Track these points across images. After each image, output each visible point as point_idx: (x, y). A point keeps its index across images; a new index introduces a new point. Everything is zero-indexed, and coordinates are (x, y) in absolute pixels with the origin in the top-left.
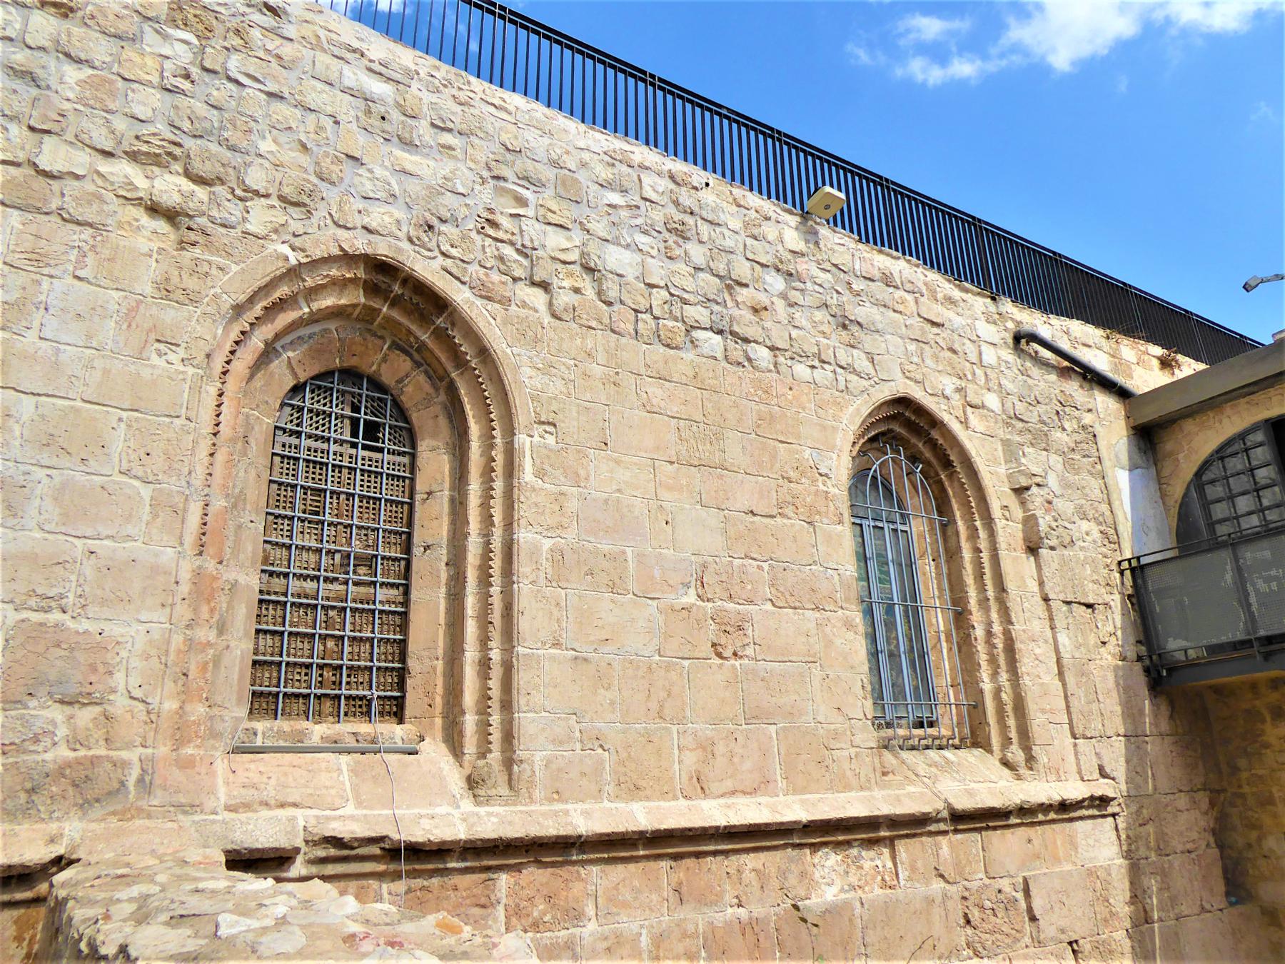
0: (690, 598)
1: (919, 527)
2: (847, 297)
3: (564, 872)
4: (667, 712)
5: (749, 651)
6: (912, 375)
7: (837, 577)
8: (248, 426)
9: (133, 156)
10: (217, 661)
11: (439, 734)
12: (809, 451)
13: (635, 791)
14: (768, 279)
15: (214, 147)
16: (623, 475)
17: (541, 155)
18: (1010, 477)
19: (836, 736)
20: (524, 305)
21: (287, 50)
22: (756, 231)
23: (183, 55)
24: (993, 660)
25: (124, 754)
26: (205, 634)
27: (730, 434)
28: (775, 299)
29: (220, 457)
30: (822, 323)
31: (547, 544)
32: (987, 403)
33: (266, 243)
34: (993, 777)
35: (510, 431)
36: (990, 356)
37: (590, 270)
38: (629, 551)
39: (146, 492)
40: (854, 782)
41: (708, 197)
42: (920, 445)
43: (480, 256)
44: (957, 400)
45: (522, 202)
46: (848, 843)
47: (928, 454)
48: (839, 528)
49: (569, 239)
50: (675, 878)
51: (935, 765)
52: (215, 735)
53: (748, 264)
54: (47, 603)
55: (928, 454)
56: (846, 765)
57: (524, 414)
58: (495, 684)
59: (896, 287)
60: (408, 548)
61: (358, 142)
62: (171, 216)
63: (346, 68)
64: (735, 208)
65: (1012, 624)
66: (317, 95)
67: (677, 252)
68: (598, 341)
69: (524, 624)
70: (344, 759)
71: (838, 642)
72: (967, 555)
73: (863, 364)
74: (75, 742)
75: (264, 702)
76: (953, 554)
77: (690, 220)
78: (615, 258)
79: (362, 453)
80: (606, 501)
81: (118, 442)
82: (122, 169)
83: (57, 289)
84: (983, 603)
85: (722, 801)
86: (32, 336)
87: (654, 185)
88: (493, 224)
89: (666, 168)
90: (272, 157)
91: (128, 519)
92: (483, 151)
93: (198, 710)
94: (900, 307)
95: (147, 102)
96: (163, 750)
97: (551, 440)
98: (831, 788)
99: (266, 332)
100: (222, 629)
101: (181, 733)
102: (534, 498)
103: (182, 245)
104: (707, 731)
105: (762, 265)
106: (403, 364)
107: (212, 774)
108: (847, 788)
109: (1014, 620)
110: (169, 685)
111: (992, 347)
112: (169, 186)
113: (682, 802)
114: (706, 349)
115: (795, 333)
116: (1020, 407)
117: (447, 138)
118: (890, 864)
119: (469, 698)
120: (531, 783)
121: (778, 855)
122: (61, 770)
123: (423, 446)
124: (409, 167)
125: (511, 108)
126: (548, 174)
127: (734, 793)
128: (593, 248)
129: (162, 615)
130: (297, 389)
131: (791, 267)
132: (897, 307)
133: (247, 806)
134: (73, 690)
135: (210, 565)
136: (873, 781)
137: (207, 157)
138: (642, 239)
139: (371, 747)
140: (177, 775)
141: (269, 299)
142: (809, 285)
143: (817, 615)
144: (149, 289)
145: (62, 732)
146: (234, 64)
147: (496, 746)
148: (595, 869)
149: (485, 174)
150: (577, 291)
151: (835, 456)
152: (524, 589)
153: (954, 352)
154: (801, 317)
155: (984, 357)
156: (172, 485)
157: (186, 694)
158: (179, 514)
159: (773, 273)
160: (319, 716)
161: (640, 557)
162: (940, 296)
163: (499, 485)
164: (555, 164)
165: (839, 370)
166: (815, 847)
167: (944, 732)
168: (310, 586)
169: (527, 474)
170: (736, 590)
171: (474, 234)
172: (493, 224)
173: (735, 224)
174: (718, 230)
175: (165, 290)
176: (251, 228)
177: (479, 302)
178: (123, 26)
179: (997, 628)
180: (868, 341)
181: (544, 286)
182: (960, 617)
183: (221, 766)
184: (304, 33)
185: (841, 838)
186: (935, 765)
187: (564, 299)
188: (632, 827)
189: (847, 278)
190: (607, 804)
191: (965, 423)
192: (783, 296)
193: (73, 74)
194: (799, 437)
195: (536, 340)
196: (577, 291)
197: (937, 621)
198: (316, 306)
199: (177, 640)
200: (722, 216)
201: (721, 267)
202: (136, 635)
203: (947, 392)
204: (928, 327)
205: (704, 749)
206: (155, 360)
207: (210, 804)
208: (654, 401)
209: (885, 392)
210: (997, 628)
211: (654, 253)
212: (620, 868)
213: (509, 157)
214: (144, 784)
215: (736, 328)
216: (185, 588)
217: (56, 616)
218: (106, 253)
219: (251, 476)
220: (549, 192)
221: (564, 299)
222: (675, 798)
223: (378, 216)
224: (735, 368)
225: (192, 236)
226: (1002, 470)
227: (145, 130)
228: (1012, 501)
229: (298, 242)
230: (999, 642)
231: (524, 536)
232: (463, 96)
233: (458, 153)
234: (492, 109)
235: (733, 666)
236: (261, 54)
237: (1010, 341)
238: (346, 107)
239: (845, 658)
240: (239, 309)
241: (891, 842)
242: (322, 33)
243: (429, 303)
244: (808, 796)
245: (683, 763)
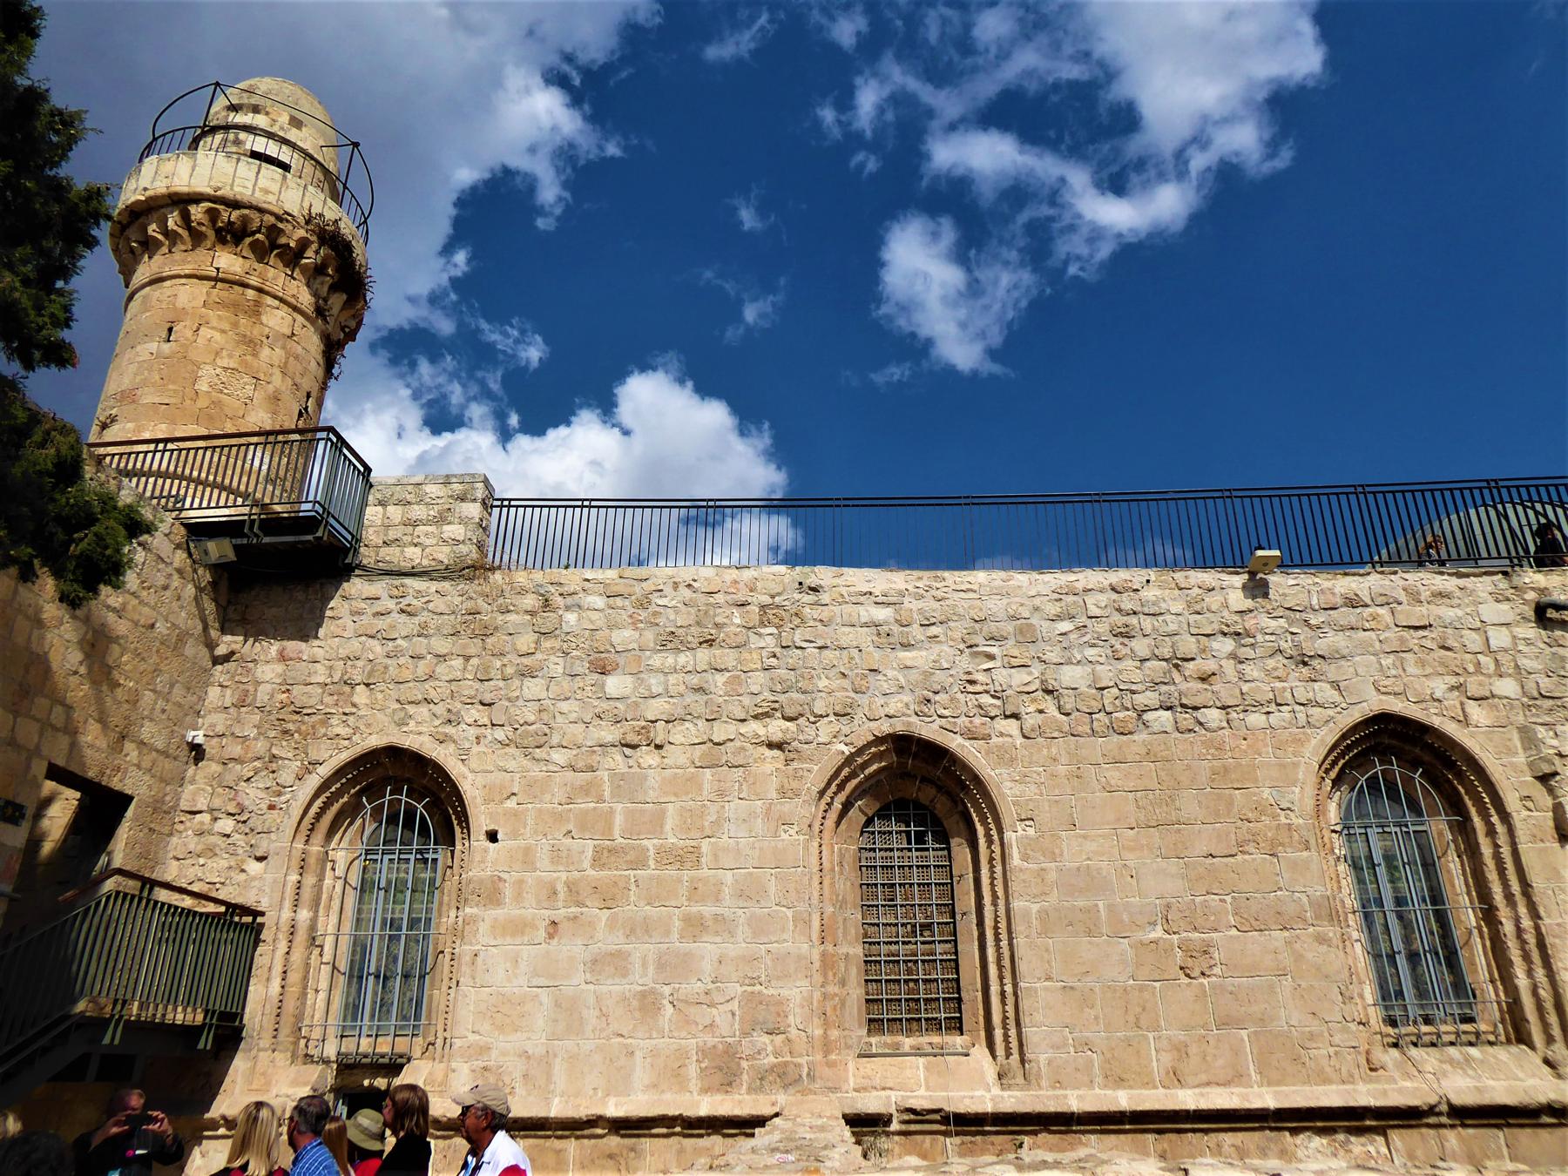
0: (1158, 933)
1: (1439, 827)
2: (1304, 633)
3: (1069, 1137)
4: (1143, 1023)
5: (1217, 970)
6: (1389, 690)
7: (1305, 899)
8: (842, 856)
9: (756, 717)
10: (843, 1003)
11: (984, 1043)
12: (1268, 791)
13: (1120, 1082)
14: (1215, 645)
15: (795, 695)
16: (1091, 846)
17: (1002, 615)
18: (1531, 765)
20: (1002, 734)
21: (825, 613)
22: (1198, 607)
23: (770, 642)
24: (1526, 957)
25: (799, 1060)
26: (832, 989)
27: (1185, 793)
28: (1223, 662)
29: (826, 882)
30: (1276, 669)
31: (1035, 908)
32: (1496, 692)
33: (833, 743)
34: (1521, 1075)
35: (1000, 832)
36: (1499, 638)
37: (1049, 692)
38: (1101, 904)
39: (789, 913)
40: (1334, 1076)
41: (1149, 594)
42: (1417, 750)
43: (965, 709)
44: (1453, 700)
45: (991, 657)
46: (1333, 1131)
47: (1427, 758)
48: (1305, 854)
49: (1030, 673)
50: (1159, 1148)
51: (1451, 1061)
52: (849, 1047)
53: (1193, 639)
54: (754, 980)
55: (1427, 758)
56: (1324, 1062)
57: (1008, 813)
58: (1010, 1008)
59: (1367, 606)
60: (953, 916)
61: (876, 657)
62: (779, 746)
63: (860, 608)
64: (1177, 592)
65: (1540, 918)
66: (847, 636)
67: (1125, 650)
68: (1059, 747)
69: (1022, 967)
70: (921, 1060)
71: (1310, 955)
72: (1486, 850)
73: (1333, 695)
74: (776, 1054)
75: (875, 1025)
76: (1471, 852)
77: (1133, 620)
78: (1071, 676)
79: (915, 854)
81: (772, 890)
82: (754, 727)
83: (734, 807)
84: (1509, 897)
85: (1197, 1091)
86: (725, 837)
87: (1095, 603)
88: (972, 682)
89: (1106, 583)
90: (828, 689)
91: (783, 930)
92: (959, 629)
93: (834, 1034)
94: (1373, 624)
95: (758, 681)
96: (819, 1057)
97: (1031, 831)
98: (1308, 1081)
99: (842, 797)
100: (843, 983)
101: (827, 1047)
102: (1022, 876)
103: (787, 762)
104: (1181, 1036)
105: (1207, 636)
106: (931, 791)
107: (846, 1070)
108: (1327, 1081)
109: (1542, 913)
110: (816, 1020)
111: (1504, 629)
112: (776, 728)
113: (1162, 1090)
114: (1156, 727)
115: (1245, 688)
116: (1546, 684)
117: (934, 630)
118: (1384, 1150)
119: (996, 1018)
120: (1039, 1076)
121: (1257, 1135)
122: (772, 1069)
123: (954, 842)
124: (909, 663)
125: (975, 587)
126: (1009, 628)
127: (1208, 1084)
128: (1049, 676)
129: (806, 982)
130: (869, 822)
131: (1239, 628)
132: (1367, 626)
133: (865, 1089)
134: (771, 1026)
135: (830, 948)
136: (1357, 1076)
137: (792, 702)
138: (1090, 653)
139: (940, 1052)
140: (827, 1071)
141: (836, 780)
142: (1260, 638)
143: (1286, 934)
144: (774, 795)
145: (770, 1048)
146: (798, 638)
147: (1015, 1051)
148: (1093, 1137)
149: (962, 646)
150: (1041, 712)
151: (1297, 790)
152: (1020, 941)
153: (1448, 649)
154: (1251, 670)
155: (1492, 642)
156: (802, 907)
157: (826, 1025)
158: (808, 923)
159: (1220, 638)
160: (910, 1033)
161: (1111, 908)
162: (1425, 595)
163: (999, 869)
164: (1014, 618)
165: (1298, 708)
166: (1295, 1132)
167: (1483, 1027)
168: (893, 948)
169: (1015, 860)
170: (1199, 922)
171: (959, 695)
172: (972, 682)
173: (1177, 607)
174: (1160, 618)
175: (782, 793)
176: (821, 740)
177: (967, 743)
178: (741, 639)
179: (1526, 923)
180: (1332, 671)
181: (1015, 716)
182: (1489, 915)
183: (851, 1066)
184: (836, 596)
185: (1319, 1124)
186: (1451, 1061)
187: (1031, 721)
188: (1113, 1108)
189: (1304, 615)
190: (1097, 1091)
191: (1465, 721)
192: (1233, 656)
193: (721, 679)
194: (1256, 780)
195: (1012, 760)
196: (1041, 712)
197: (1466, 916)
198: (867, 772)
199: (817, 995)
200: (1163, 605)
201: (1166, 652)
202: (796, 993)
203: (1438, 695)
204: (1406, 634)
205: (1179, 1050)
206: (784, 836)
207: (845, 1088)
208: (1113, 782)
209: (1356, 715)
210: (1526, 923)
211: (1102, 660)
212: (1113, 1137)
213: (977, 626)
215: (1184, 701)
216: (817, 965)
217: (758, 987)
218: (751, 780)
219: (846, 884)
220: (1011, 642)
221: (1031, 721)
222: (1155, 1087)
223: (894, 705)
224: (1187, 736)
225: (792, 756)
226: (1521, 759)
227: (758, 699)
228: (1538, 791)
229: (848, 740)
230: (1531, 938)
231: (1017, 904)
232: (939, 594)
233: (942, 638)
234: (962, 595)
235: (1202, 984)
236: (811, 623)
237: (1531, 614)
238: (865, 637)
239: (1318, 969)
240: (822, 793)
241: (1382, 1131)
242: (844, 591)
243: (934, 753)
244: (1284, 1088)
245: (1158, 1062)
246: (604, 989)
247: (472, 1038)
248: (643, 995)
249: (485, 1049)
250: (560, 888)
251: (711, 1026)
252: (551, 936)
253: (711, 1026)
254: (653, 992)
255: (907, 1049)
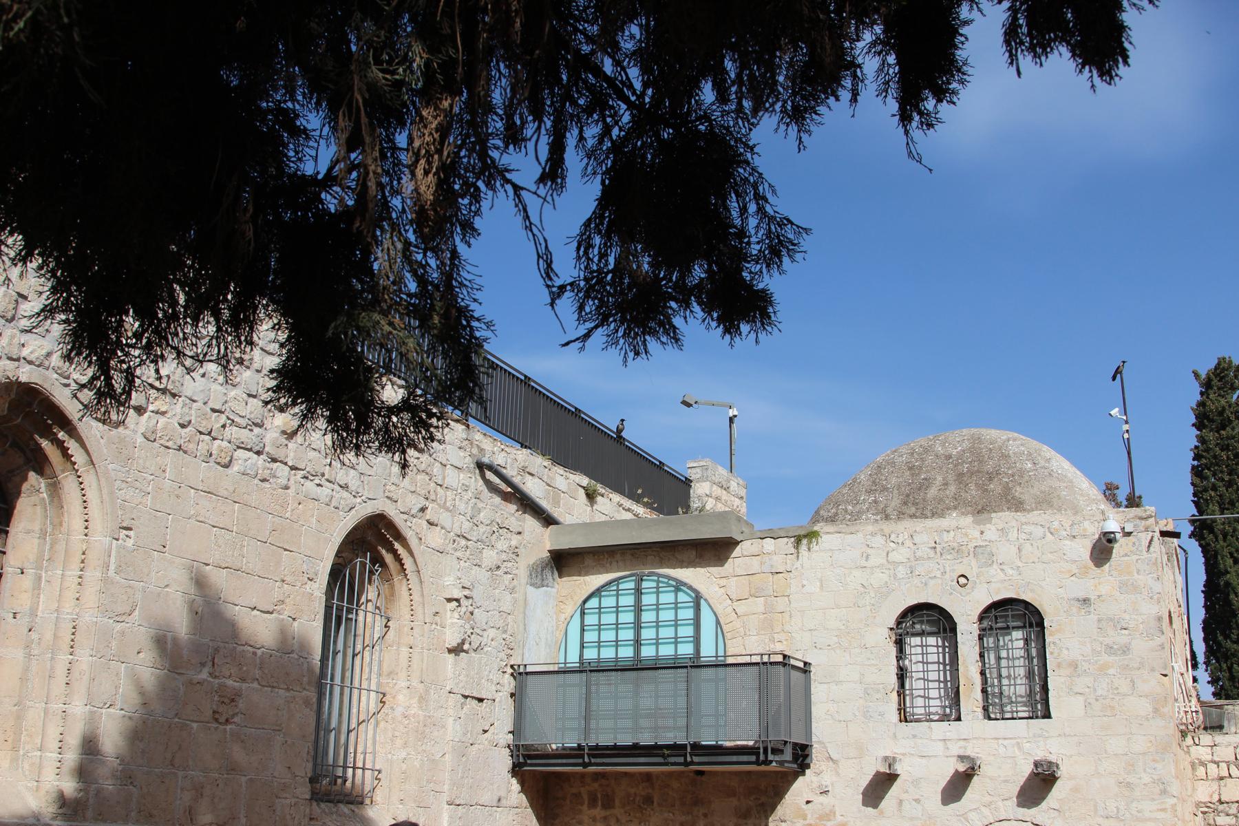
0: (204, 675)
19: (285, 787)
80: (159, 594)
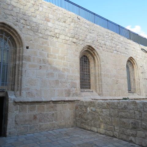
0: (114, 78)
21: (81, 23)
36: (139, 52)
41: (114, 35)
78: (107, 43)
82: (71, 39)
112: (75, 40)
160: (85, 89)
181: (102, 47)
214: (80, 95)
246: (50, 79)
247: (26, 87)
248: (56, 81)
249: (28, 89)
250: (41, 60)
251: (66, 86)
252: (40, 69)
253: (66, 86)
254: (58, 80)
255: (85, 91)
